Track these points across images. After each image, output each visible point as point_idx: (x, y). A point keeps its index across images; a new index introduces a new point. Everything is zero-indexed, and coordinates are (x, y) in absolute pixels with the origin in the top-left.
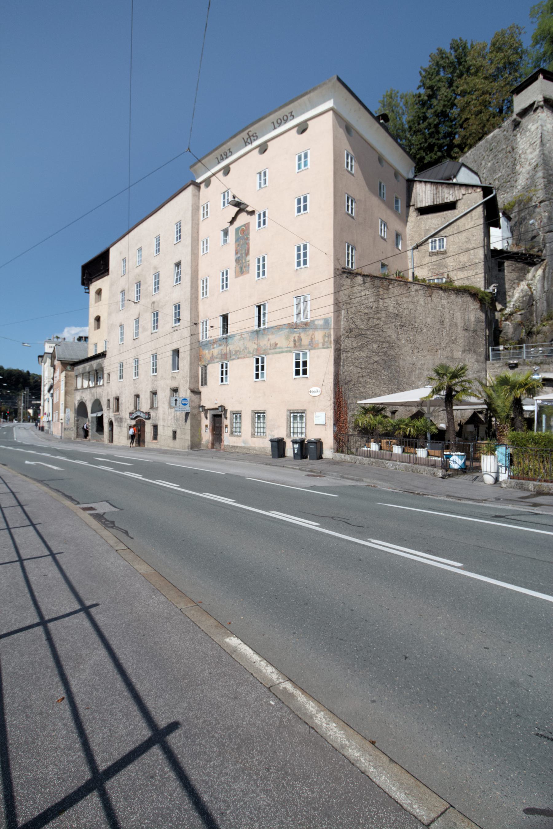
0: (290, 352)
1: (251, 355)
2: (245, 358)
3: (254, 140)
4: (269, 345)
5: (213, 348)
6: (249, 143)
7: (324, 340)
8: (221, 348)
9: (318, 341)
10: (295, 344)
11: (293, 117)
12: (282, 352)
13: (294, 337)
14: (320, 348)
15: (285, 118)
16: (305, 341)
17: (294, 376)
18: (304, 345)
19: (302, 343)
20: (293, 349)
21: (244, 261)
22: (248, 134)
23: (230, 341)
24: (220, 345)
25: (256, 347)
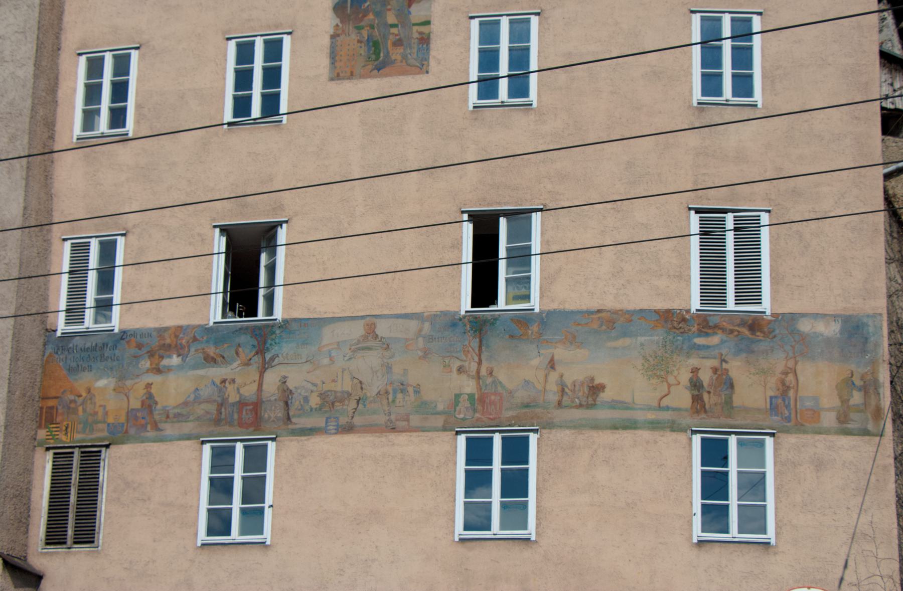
0: (674, 427)
1: (440, 421)
2: (394, 429)
4: (552, 386)
5: (158, 371)
7: (844, 401)
8: (217, 373)
9: (816, 399)
10: (697, 399)
12: (630, 425)
13: (695, 371)
14: (827, 432)
16: (751, 390)
17: (697, 532)
18: (747, 410)
19: (737, 401)
20: (687, 420)
21: (391, 19)
23: (285, 348)
24: (210, 361)
25: (470, 387)
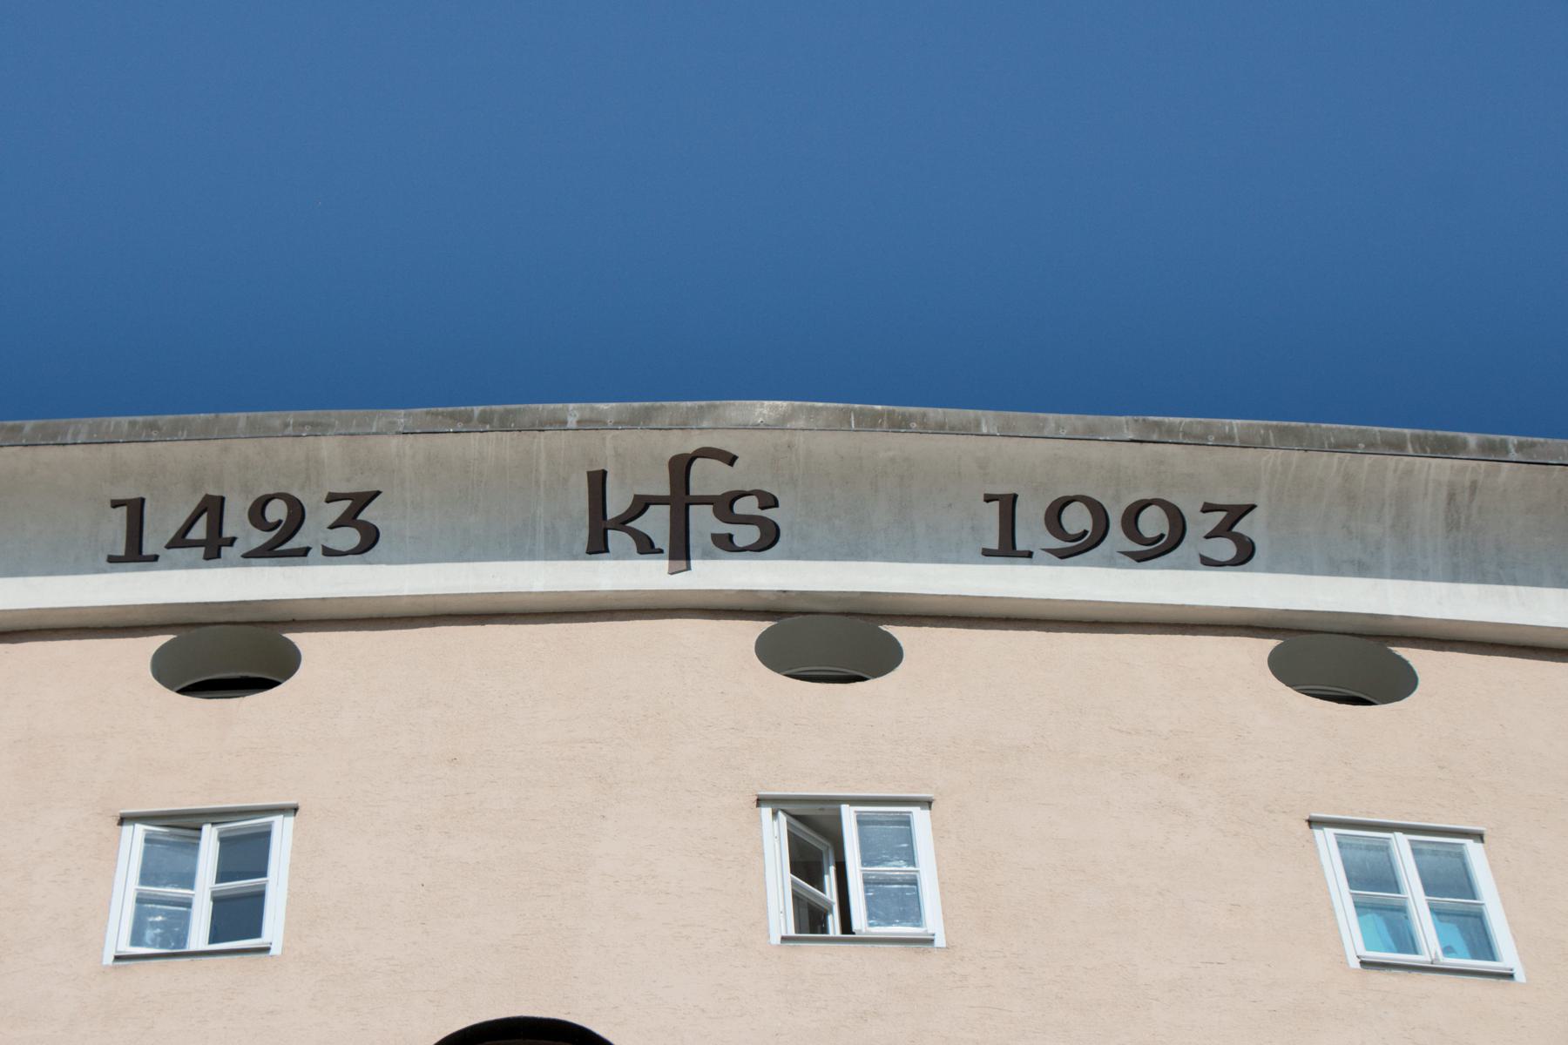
3: (726, 544)
6: (646, 547)
11: (1245, 555)
15: (1153, 523)
22: (681, 467)
